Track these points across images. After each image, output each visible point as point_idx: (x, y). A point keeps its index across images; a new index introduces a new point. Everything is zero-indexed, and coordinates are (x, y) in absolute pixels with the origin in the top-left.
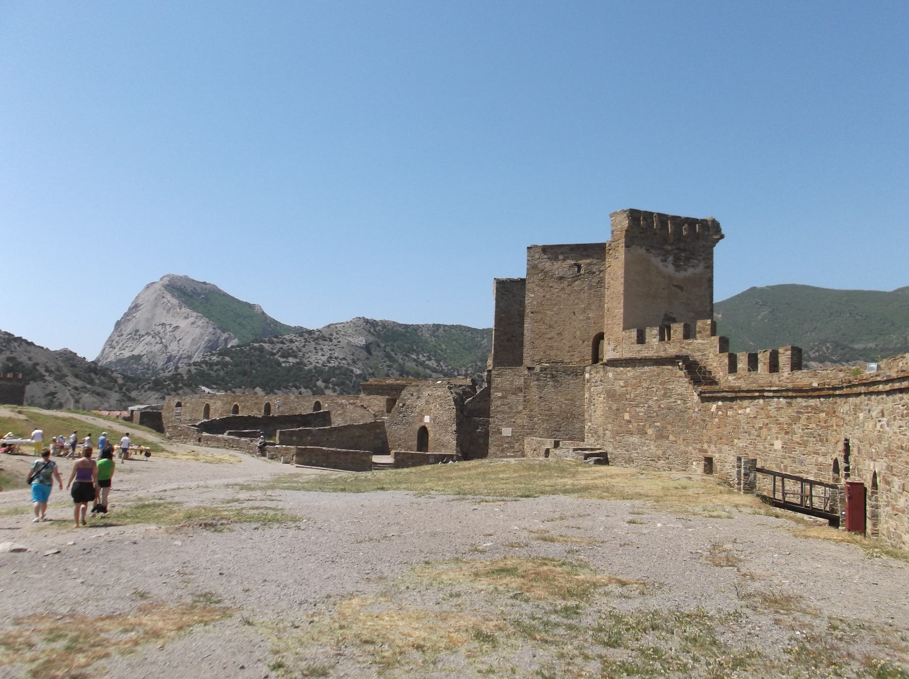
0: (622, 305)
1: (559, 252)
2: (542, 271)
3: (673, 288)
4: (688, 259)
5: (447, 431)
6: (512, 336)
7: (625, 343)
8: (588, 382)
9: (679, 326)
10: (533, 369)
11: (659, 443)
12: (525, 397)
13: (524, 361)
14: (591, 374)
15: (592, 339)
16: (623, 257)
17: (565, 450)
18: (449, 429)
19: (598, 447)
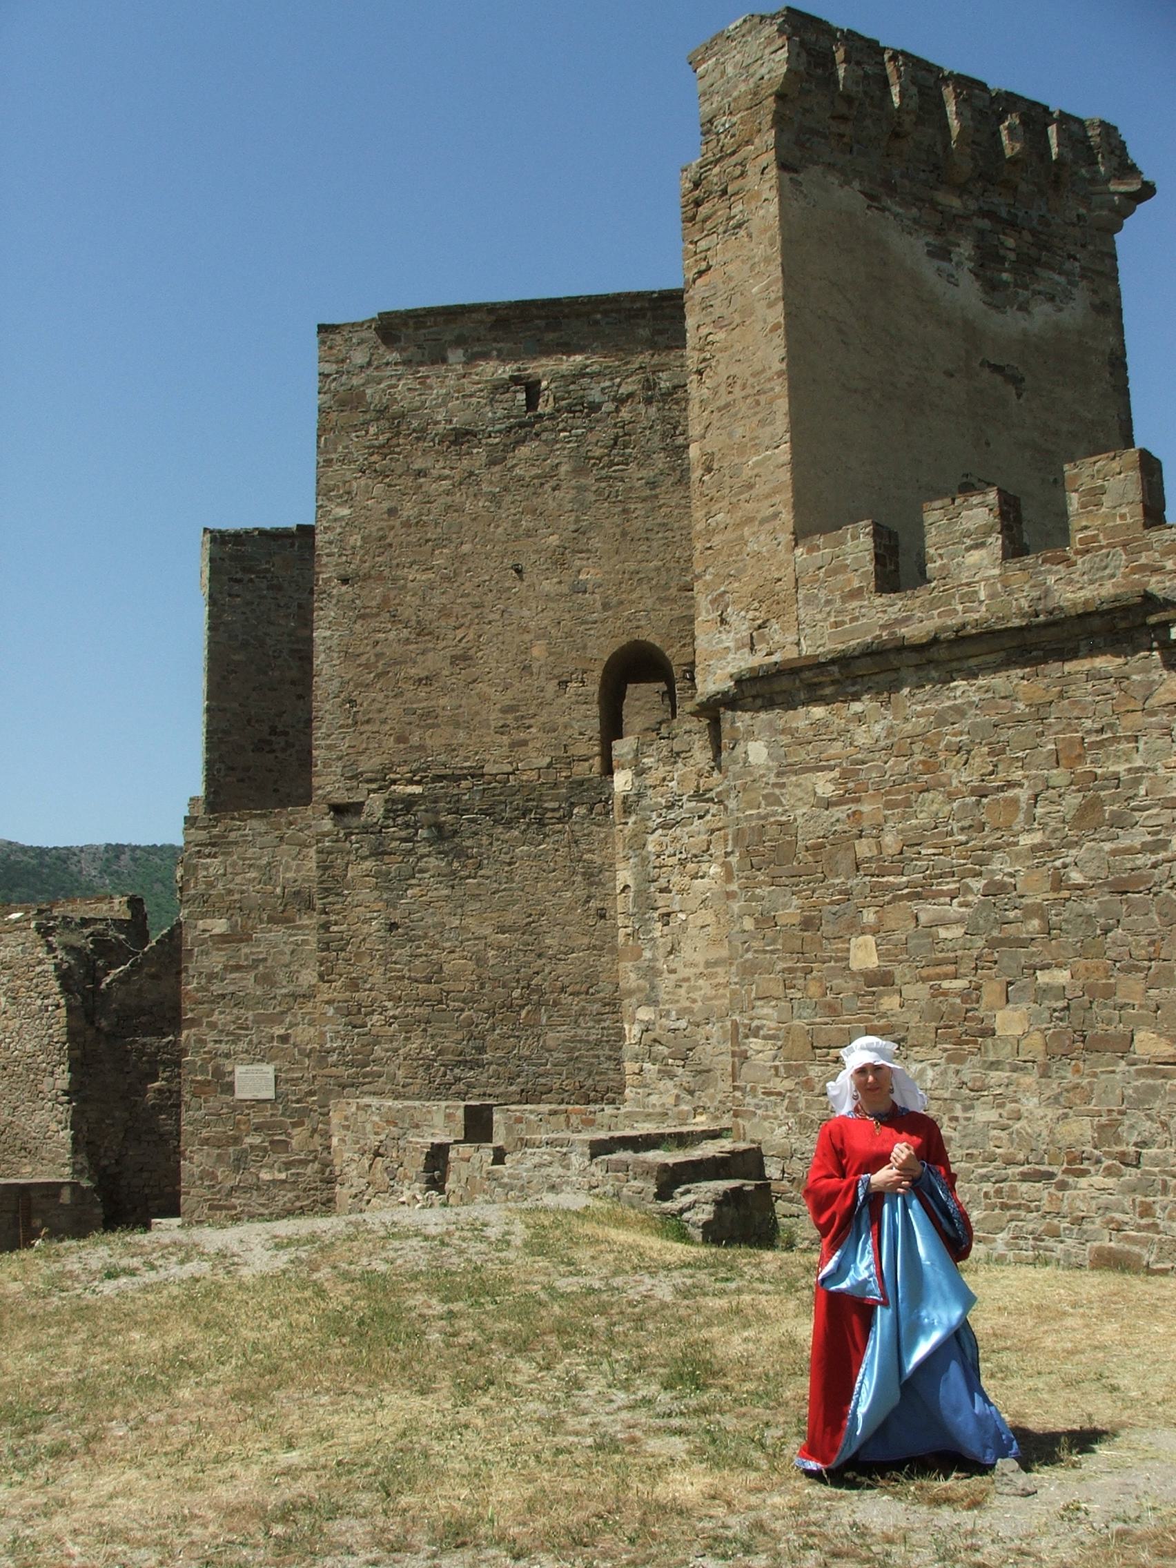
0: (781, 423)
1: (448, 337)
2: (382, 412)
3: (986, 373)
4: (1027, 265)
5: (37, 1095)
6: (273, 731)
7: (810, 600)
8: (627, 810)
9: (1115, 465)
10: (356, 808)
11: (1071, 1078)
12: (325, 927)
13: (316, 781)
14: (640, 773)
15: (598, 673)
16: (774, 208)
17: (544, 1154)
18: (44, 1087)
19: (701, 1123)
